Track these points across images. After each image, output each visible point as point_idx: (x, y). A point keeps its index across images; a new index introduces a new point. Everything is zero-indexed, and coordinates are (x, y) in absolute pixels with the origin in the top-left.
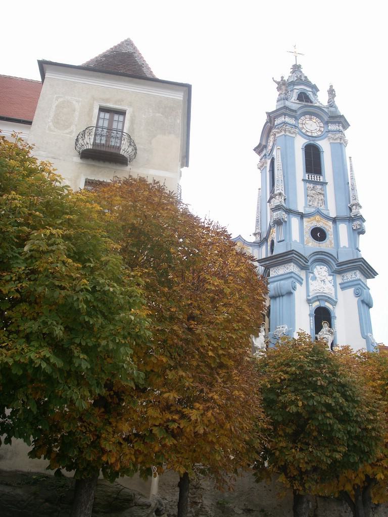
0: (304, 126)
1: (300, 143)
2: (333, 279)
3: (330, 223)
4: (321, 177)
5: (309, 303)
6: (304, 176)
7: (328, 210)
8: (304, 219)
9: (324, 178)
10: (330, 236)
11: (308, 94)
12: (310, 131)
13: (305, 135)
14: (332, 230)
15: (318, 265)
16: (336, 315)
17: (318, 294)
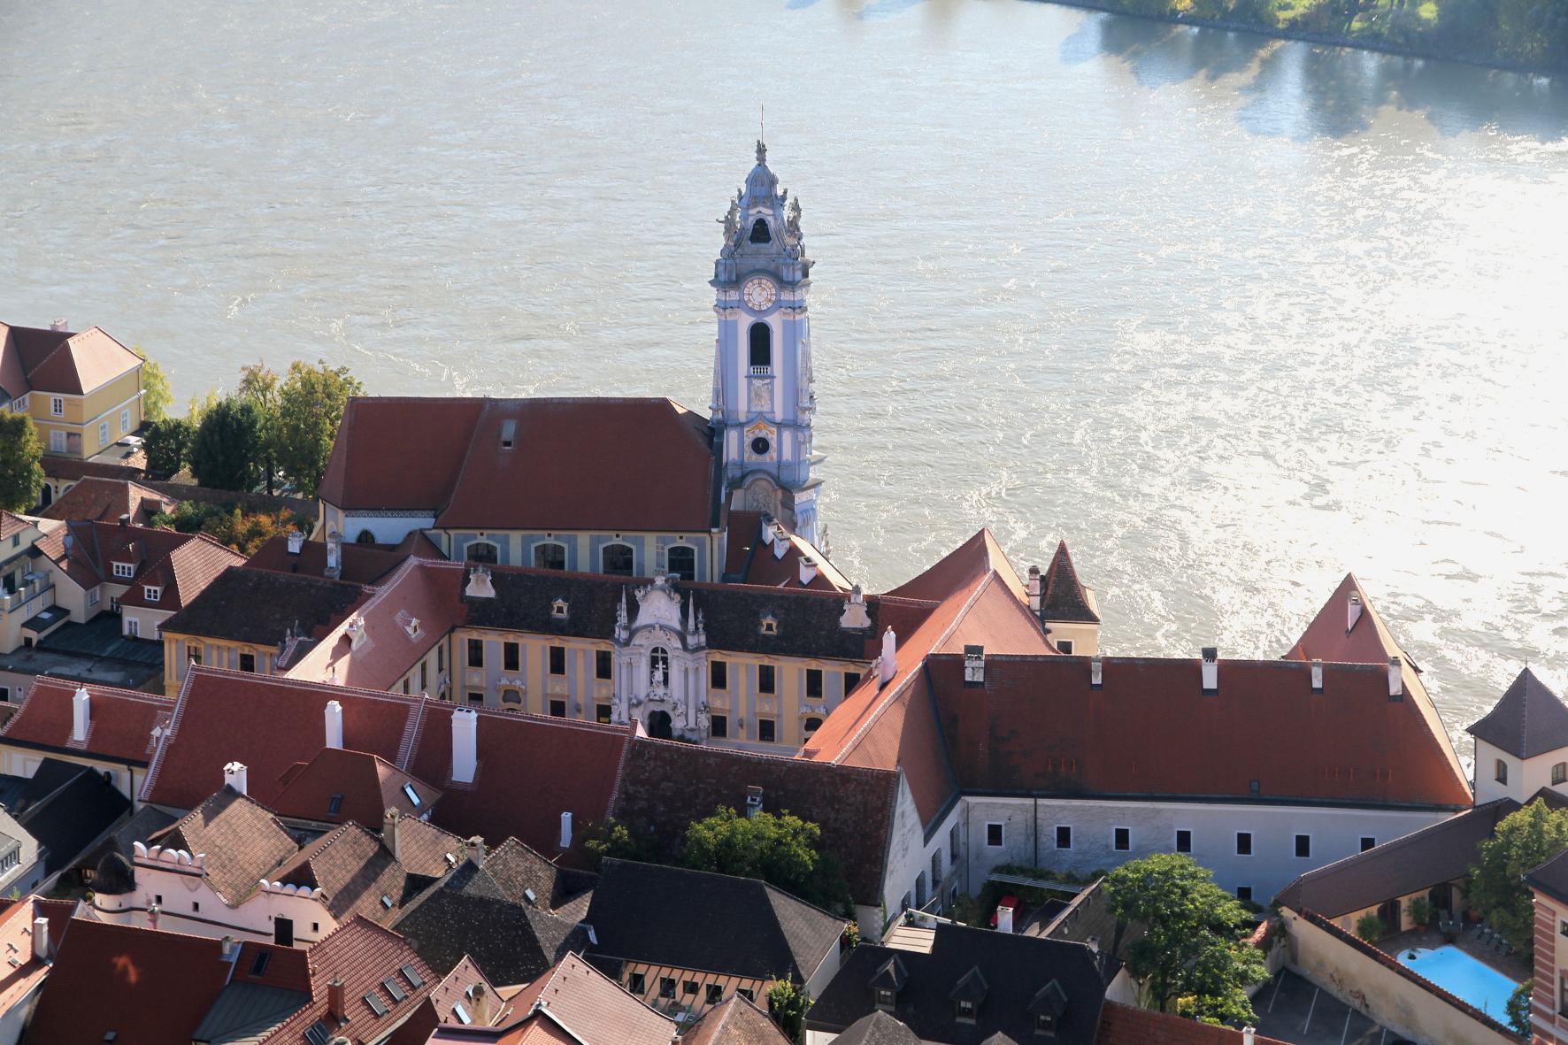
1: (745, 322)
3: (775, 430)
6: (749, 371)
9: (772, 371)
13: (752, 311)
14: (775, 437)
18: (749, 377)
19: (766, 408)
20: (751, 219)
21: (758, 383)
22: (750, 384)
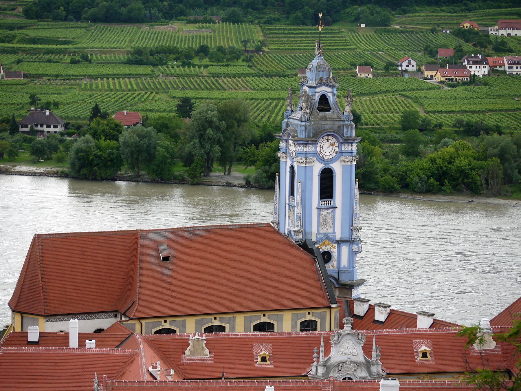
0: (321, 149)
1: (318, 167)
3: (336, 245)
4: (332, 201)
6: (319, 203)
11: (327, 97)
13: (322, 160)
18: (319, 208)
19: (330, 230)
20: (317, 95)
21: (324, 212)
22: (319, 214)
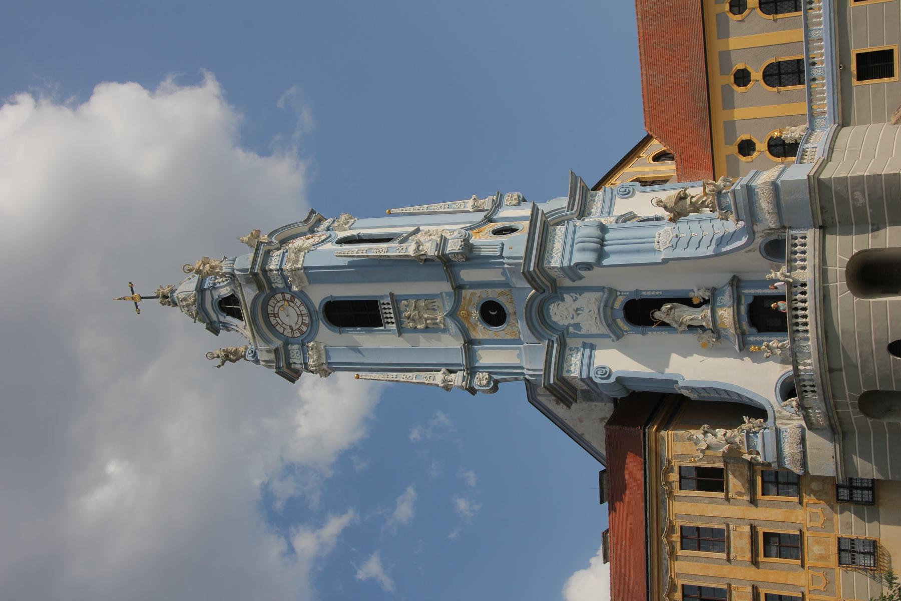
1: (326, 334)
2: (568, 293)
5: (623, 335)
7: (441, 293)
8: (472, 338)
9: (382, 297)
10: (492, 294)
12: (300, 318)
13: (313, 327)
14: (478, 292)
15: (550, 317)
16: (633, 289)
17: (604, 324)
